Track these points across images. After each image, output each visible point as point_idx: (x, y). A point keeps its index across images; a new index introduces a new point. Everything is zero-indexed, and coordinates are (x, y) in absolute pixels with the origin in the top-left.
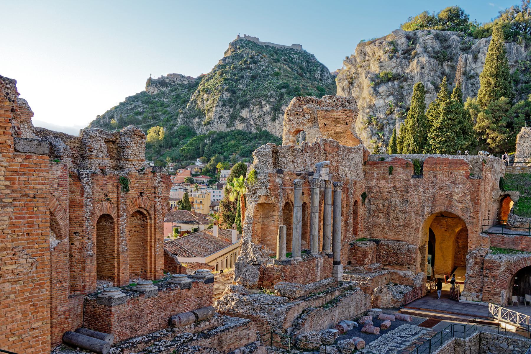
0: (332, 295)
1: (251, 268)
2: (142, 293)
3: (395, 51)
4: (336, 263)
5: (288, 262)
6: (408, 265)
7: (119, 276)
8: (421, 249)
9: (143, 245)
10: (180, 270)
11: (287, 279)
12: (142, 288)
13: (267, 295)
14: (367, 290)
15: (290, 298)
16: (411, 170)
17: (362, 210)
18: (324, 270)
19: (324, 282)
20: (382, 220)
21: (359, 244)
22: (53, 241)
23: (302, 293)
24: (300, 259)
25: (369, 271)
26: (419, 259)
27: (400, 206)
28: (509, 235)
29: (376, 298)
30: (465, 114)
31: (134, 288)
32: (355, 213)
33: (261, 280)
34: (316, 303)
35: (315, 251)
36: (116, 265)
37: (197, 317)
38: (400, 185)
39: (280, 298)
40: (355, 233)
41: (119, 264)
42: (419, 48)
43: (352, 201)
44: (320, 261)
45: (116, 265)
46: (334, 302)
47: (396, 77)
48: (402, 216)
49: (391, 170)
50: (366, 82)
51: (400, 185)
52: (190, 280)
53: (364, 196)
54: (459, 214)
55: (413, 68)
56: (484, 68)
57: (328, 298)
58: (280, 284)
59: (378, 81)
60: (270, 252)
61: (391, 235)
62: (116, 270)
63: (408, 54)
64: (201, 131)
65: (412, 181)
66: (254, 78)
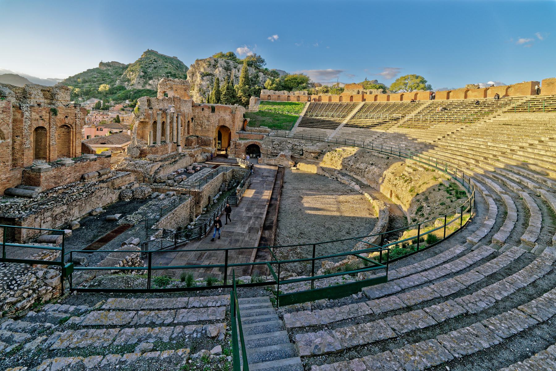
0: (174, 159)
1: (135, 149)
2: (63, 165)
4: (178, 146)
5: (154, 146)
7: (49, 157)
8: (215, 139)
9: (67, 141)
10: (93, 152)
11: (154, 153)
12: (64, 162)
13: (143, 161)
14: (192, 156)
15: (154, 161)
16: (211, 110)
17: (191, 124)
18: (172, 149)
19: (172, 153)
20: (200, 128)
21: (190, 138)
23: (160, 159)
24: (160, 145)
25: (194, 148)
26: (214, 143)
27: (206, 123)
29: (196, 159)
31: (59, 162)
32: (188, 125)
33: (141, 154)
35: (168, 141)
36: (48, 152)
37: (99, 173)
38: (206, 115)
39: (149, 162)
40: (188, 133)
41: (50, 151)
44: (170, 145)
45: (48, 152)
48: (207, 127)
51: (206, 115)
52: (96, 157)
54: (228, 126)
57: (173, 160)
58: (150, 156)
60: (146, 142)
61: (204, 134)
62: (48, 154)
65: (211, 114)
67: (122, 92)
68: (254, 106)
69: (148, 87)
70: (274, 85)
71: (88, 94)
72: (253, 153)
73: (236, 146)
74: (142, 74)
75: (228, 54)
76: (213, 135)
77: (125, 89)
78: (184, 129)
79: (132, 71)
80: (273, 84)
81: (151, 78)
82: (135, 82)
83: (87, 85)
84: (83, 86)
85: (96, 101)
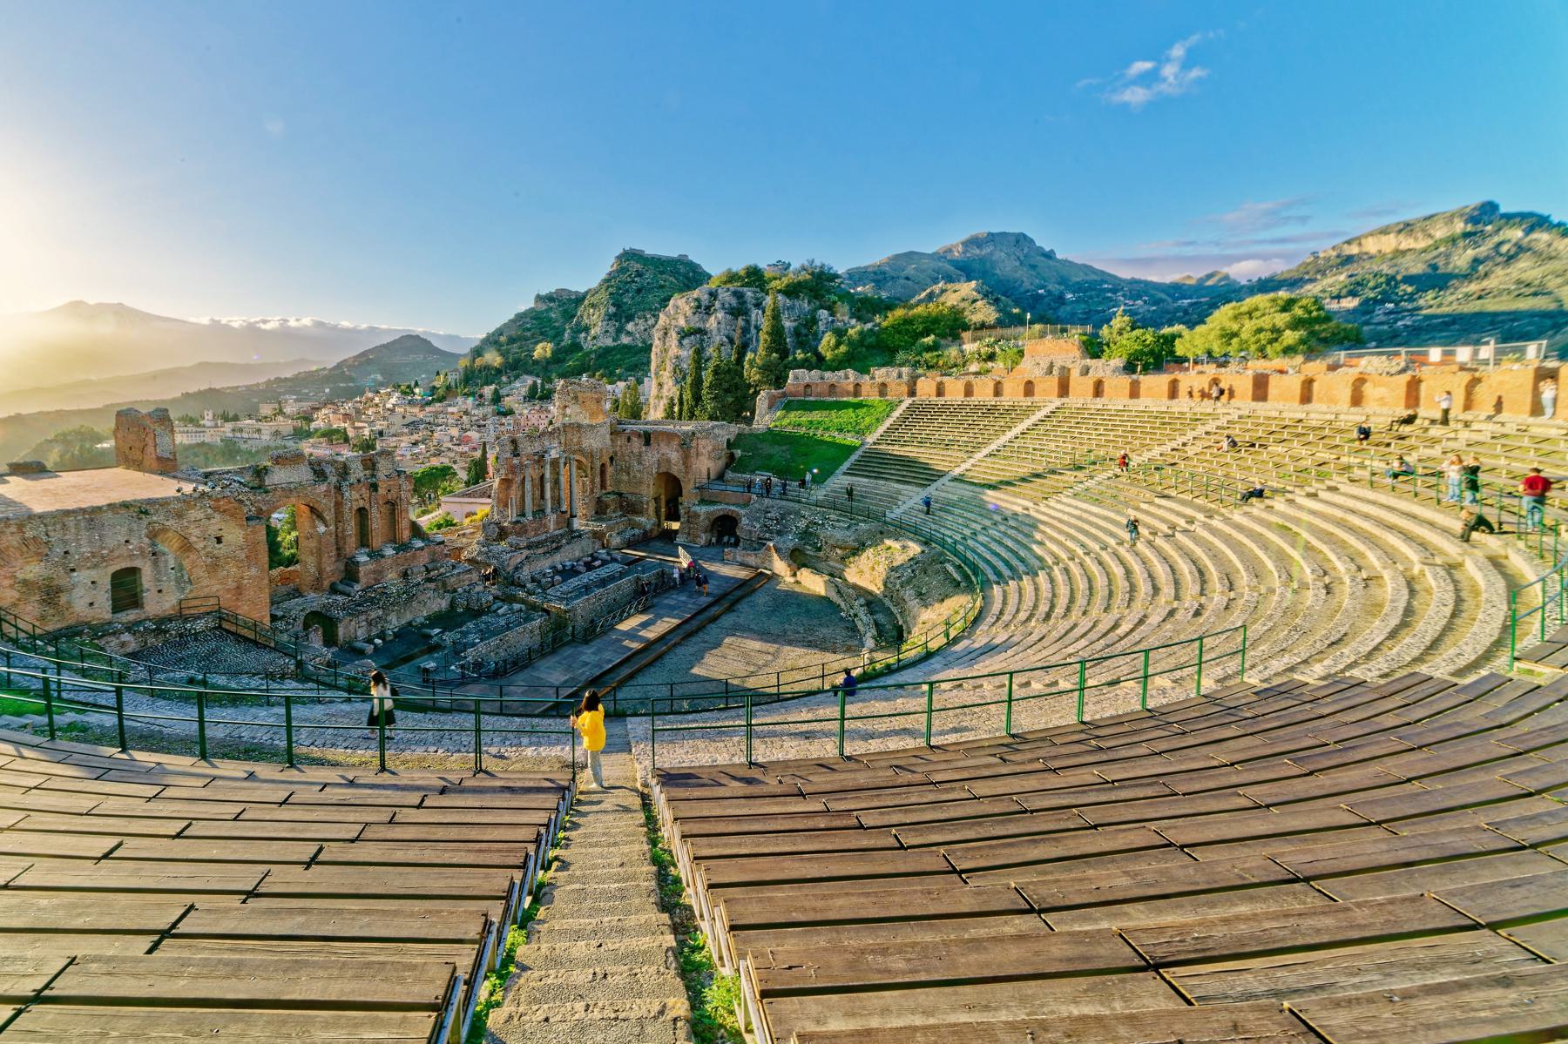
3: (699, 307)
4: (573, 516)
6: (639, 512)
11: (518, 534)
15: (517, 548)
17: (610, 470)
18: (557, 523)
20: (625, 478)
22: (322, 529)
32: (603, 472)
34: (540, 551)
40: (603, 486)
42: (717, 304)
43: (598, 465)
49: (629, 439)
53: (611, 459)
55: (712, 323)
58: (512, 539)
59: (684, 334)
61: (632, 490)
64: (588, 345)
66: (639, 291)
69: (625, 340)
70: (843, 348)
74: (612, 310)
76: (648, 491)
78: (592, 482)
79: (593, 306)
80: (838, 345)
81: (630, 318)
82: (597, 330)
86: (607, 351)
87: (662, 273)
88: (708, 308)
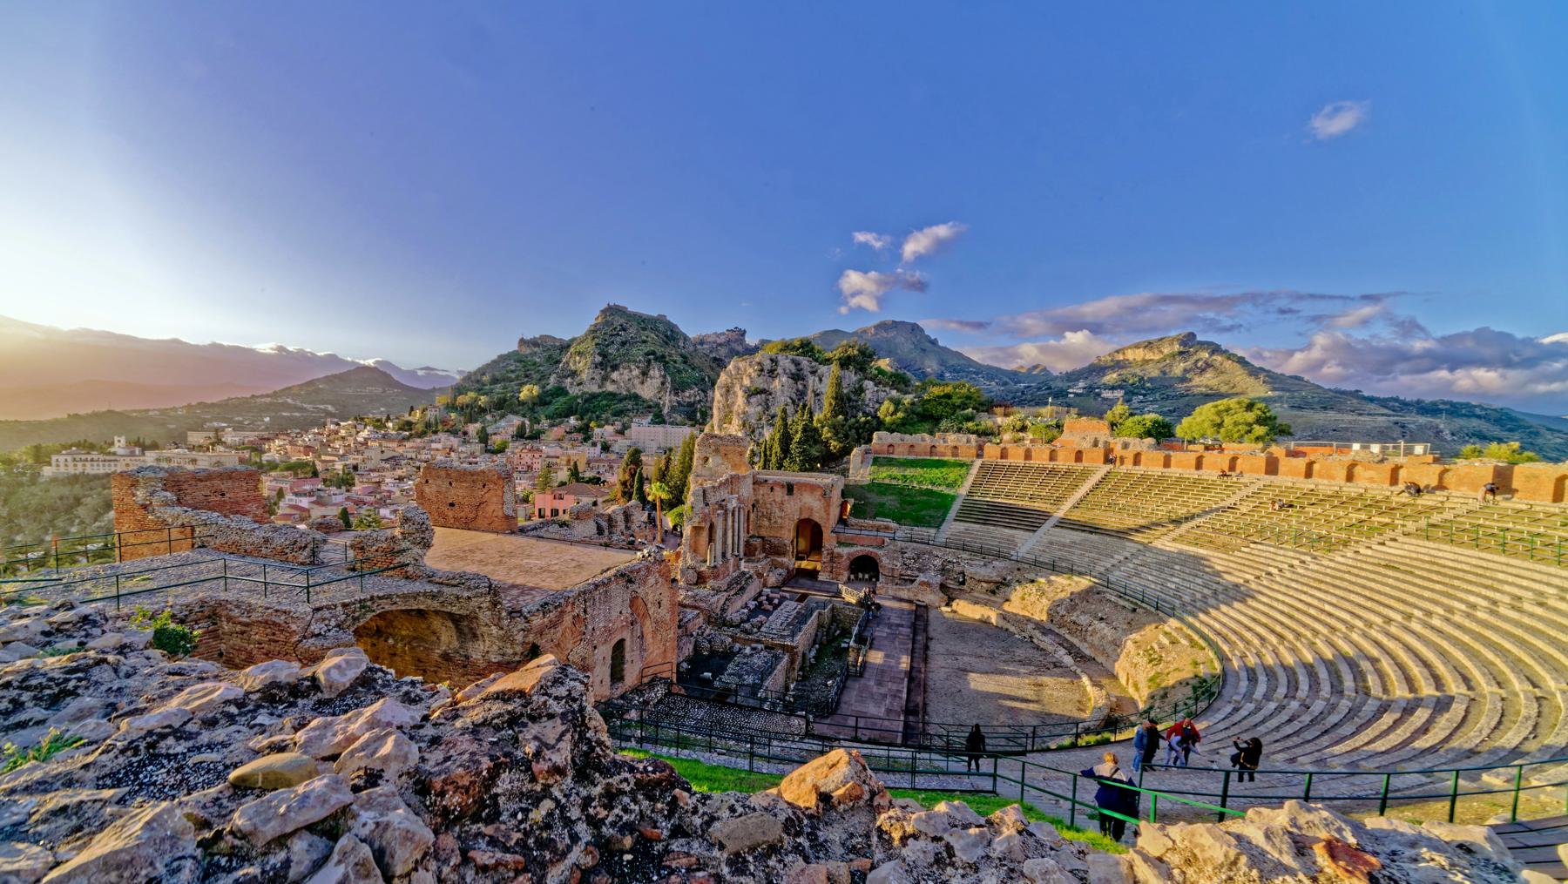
0: (739, 584)
6: (783, 554)
11: (716, 577)
13: (703, 591)
15: (718, 591)
17: (752, 516)
20: (766, 523)
28: (850, 532)
30: (816, 430)
38: (778, 499)
42: (780, 370)
46: (742, 589)
47: (763, 391)
50: (740, 393)
51: (778, 499)
55: (776, 385)
56: (827, 389)
58: (711, 583)
59: (750, 394)
63: (772, 373)
64: (574, 391)
66: (623, 344)
67: (562, 399)
68: (859, 469)
69: (610, 388)
70: (900, 415)
71: (503, 406)
72: (864, 572)
73: (833, 557)
74: (598, 359)
75: (797, 344)
76: (787, 535)
77: (567, 393)
79: (580, 353)
80: (894, 413)
81: (615, 368)
82: (585, 378)
83: (498, 388)
84: (491, 391)
85: (516, 420)
86: (594, 396)
87: (644, 329)
88: (771, 371)
